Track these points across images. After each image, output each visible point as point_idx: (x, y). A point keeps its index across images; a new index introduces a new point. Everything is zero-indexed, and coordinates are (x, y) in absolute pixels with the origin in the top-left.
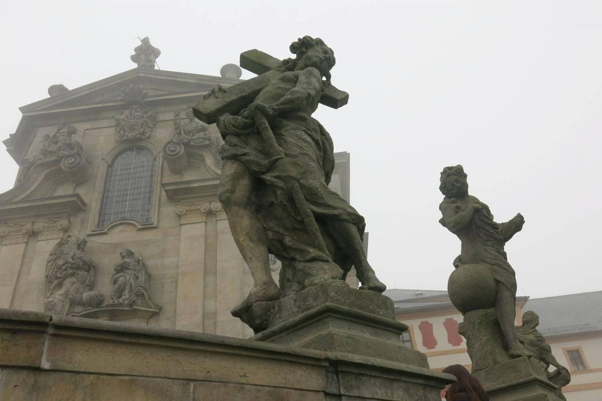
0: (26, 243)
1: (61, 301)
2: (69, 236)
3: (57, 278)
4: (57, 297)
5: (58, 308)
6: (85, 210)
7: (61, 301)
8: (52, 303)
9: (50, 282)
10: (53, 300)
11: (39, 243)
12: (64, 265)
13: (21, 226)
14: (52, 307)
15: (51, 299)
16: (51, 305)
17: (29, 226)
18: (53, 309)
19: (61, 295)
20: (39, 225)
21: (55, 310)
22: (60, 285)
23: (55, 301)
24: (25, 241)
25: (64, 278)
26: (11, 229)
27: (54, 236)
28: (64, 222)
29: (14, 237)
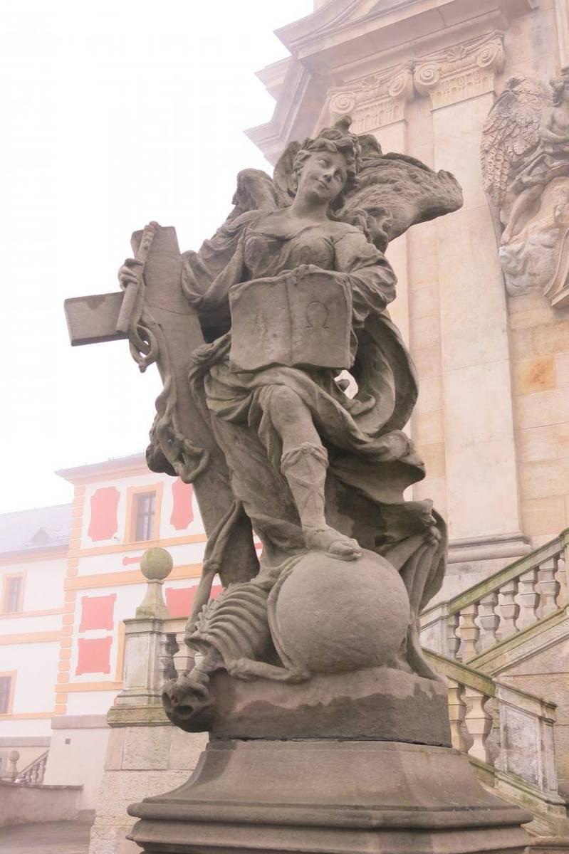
0: (404, 121)
1: (545, 246)
2: (514, 83)
3: (518, 191)
4: (535, 236)
5: (540, 265)
6: (536, 9)
7: (545, 246)
8: (521, 256)
9: (502, 205)
10: (523, 246)
11: (436, 115)
12: (528, 152)
13: (383, 82)
14: (519, 268)
15: (515, 247)
16: (518, 261)
17: (403, 79)
18: (523, 272)
19: (545, 230)
20: (428, 70)
21: (530, 274)
22: (532, 207)
23: (529, 248)
24: (401, 117)
25: (544, 185)
26: (360, 96)
27: (472, 91)
28: (492, 49)
29: (369, 113)
